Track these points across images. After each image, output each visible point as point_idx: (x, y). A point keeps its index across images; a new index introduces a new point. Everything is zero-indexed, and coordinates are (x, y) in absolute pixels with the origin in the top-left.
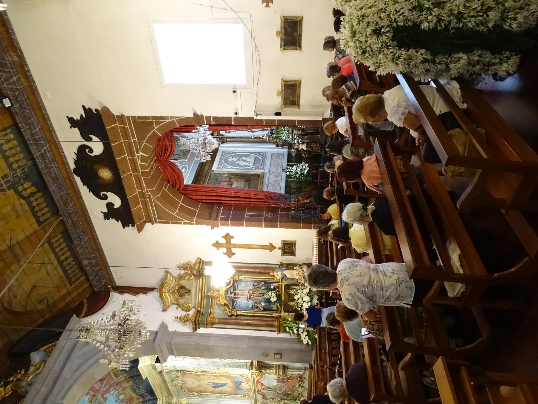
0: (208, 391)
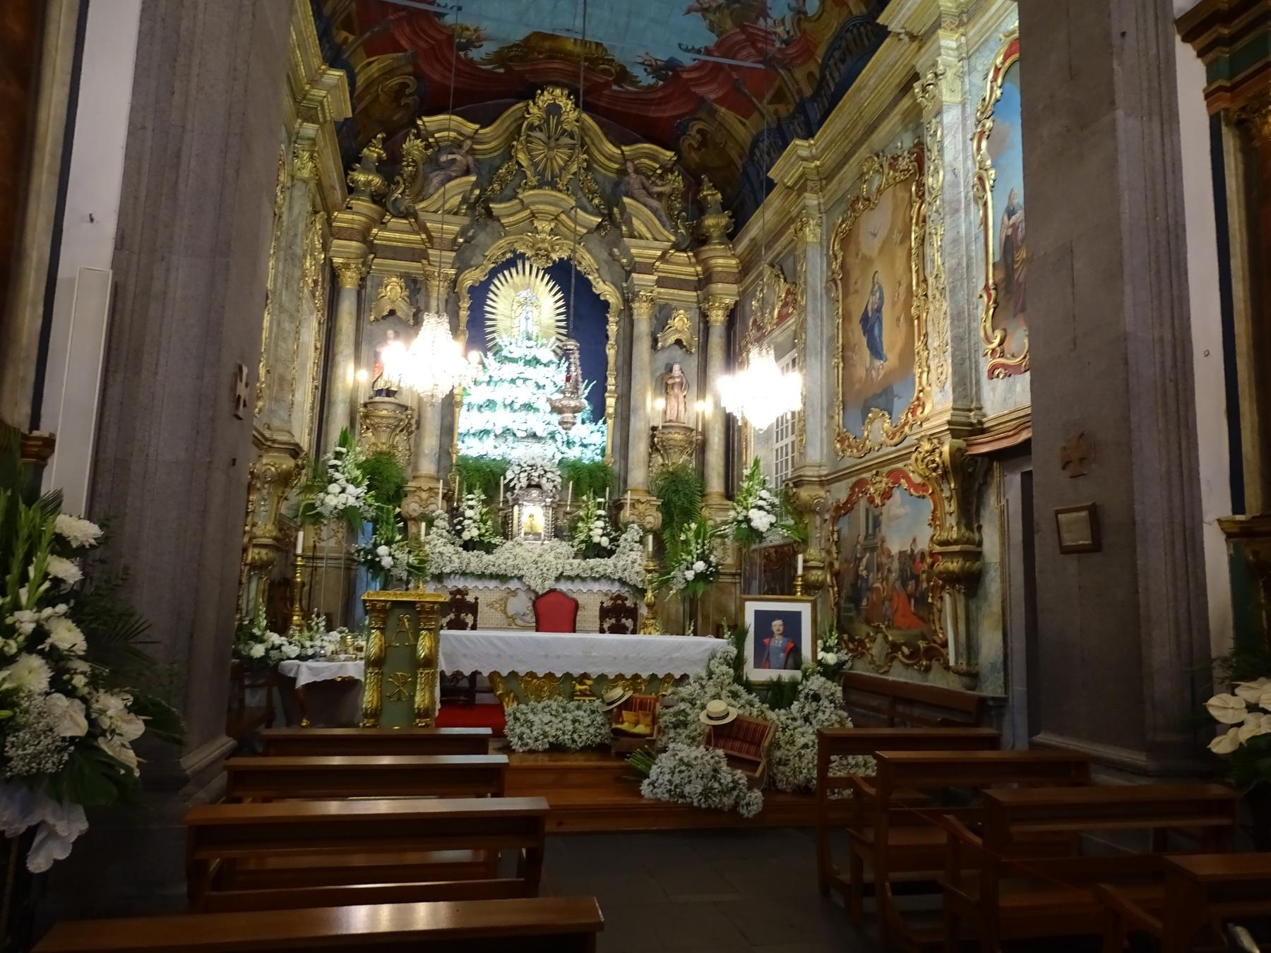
0: (850, 299)
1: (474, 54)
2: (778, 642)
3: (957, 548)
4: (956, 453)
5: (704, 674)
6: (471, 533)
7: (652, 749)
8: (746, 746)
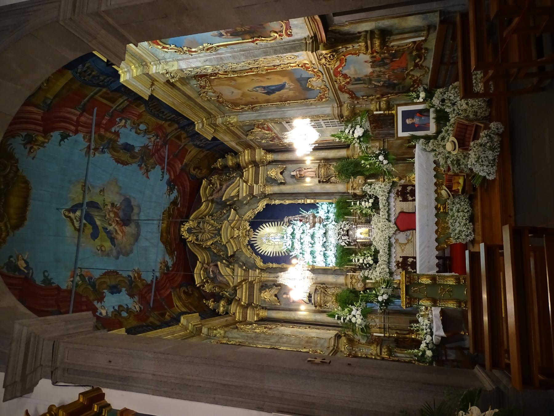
0: (260, 100)
1: (170, 264)
2: (416, 120)
3: (369, 42)
4: (326, 47)
5: (433, 153)
6: (370, 260)
7: (471, 175)
8: (468, 132)
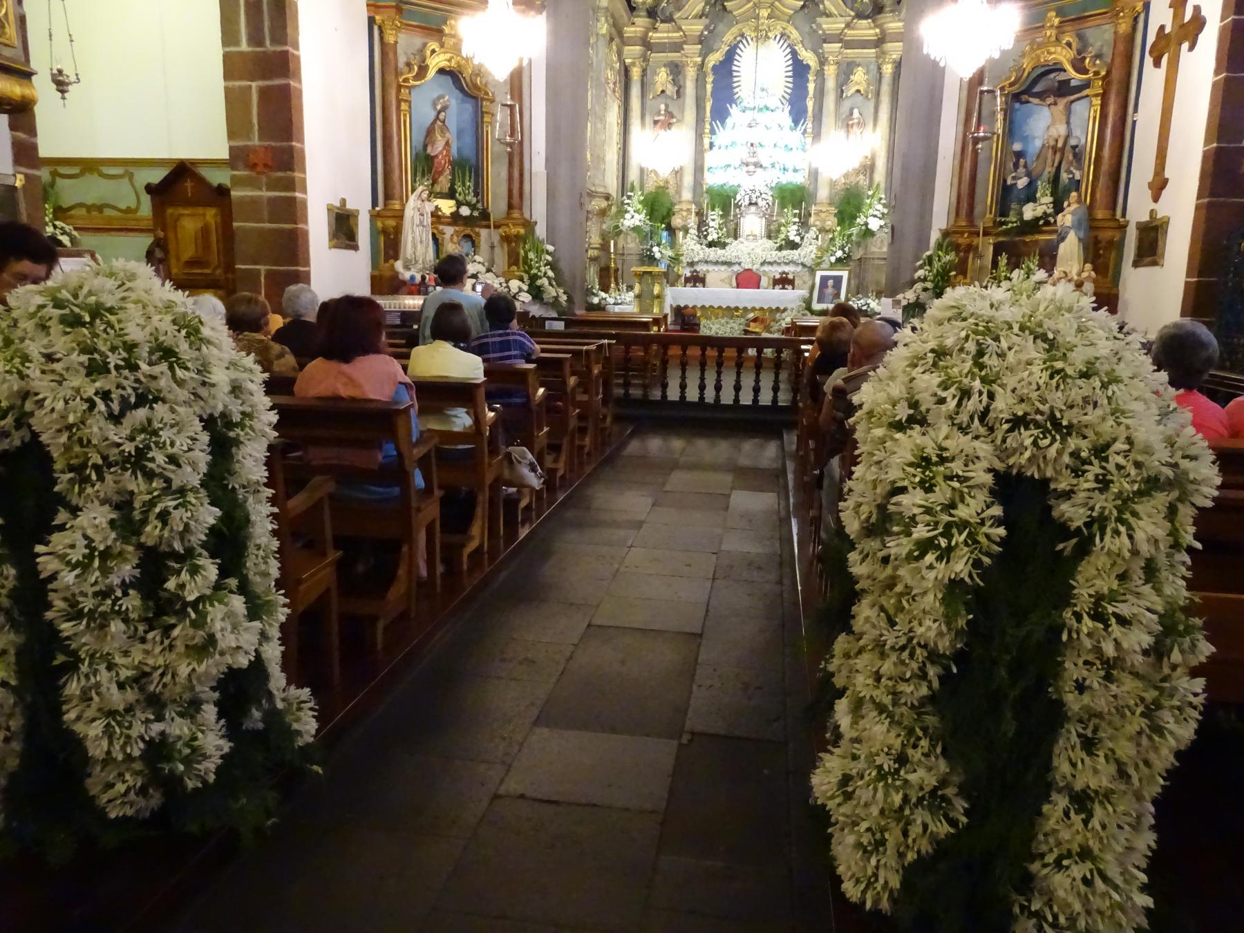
2: (830, 291)
